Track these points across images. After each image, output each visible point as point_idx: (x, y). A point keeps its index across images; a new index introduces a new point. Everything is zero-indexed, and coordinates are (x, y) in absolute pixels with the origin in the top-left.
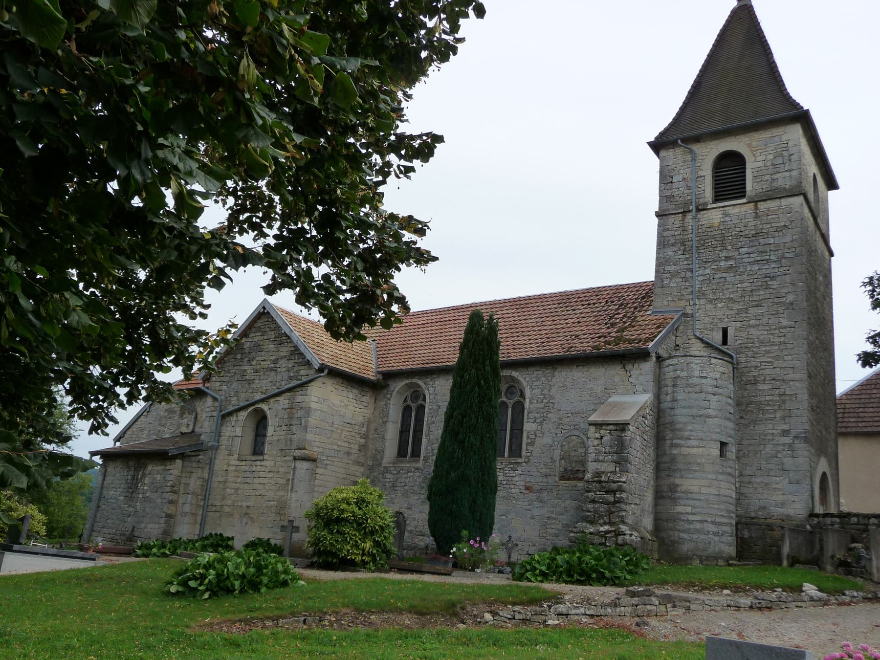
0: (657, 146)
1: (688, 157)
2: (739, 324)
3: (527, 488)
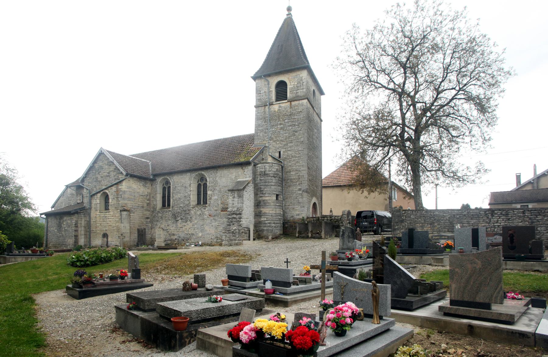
0: (255, 78)
1: (266, 83)
3: (210, 215)
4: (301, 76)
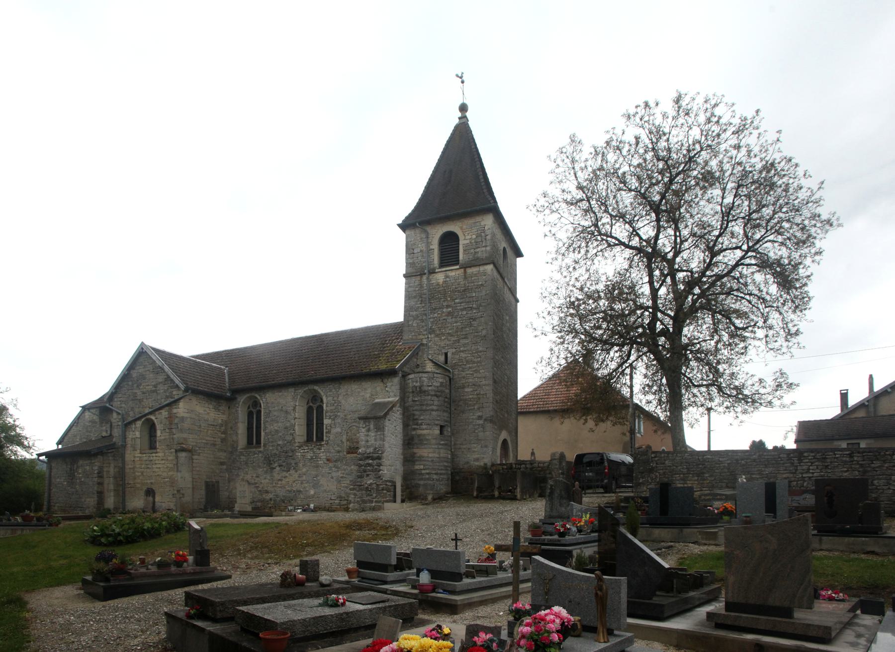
0: (404, 226)
1: (424, 236)
2: (454, 350)
3: (328, 460)
4: (482, 223)
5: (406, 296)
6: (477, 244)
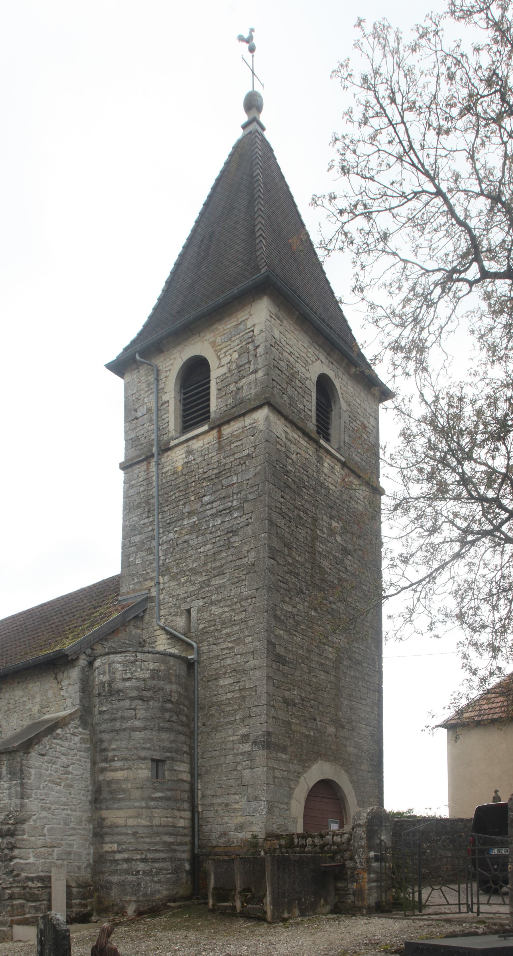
0: (120, 367)
2: (201, 603)
4: (249, 324)
5: (125, 509)
6: (240, 371)
